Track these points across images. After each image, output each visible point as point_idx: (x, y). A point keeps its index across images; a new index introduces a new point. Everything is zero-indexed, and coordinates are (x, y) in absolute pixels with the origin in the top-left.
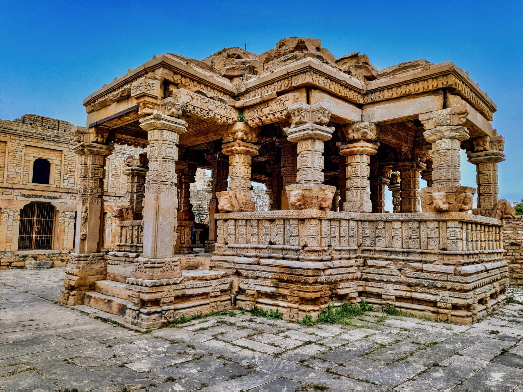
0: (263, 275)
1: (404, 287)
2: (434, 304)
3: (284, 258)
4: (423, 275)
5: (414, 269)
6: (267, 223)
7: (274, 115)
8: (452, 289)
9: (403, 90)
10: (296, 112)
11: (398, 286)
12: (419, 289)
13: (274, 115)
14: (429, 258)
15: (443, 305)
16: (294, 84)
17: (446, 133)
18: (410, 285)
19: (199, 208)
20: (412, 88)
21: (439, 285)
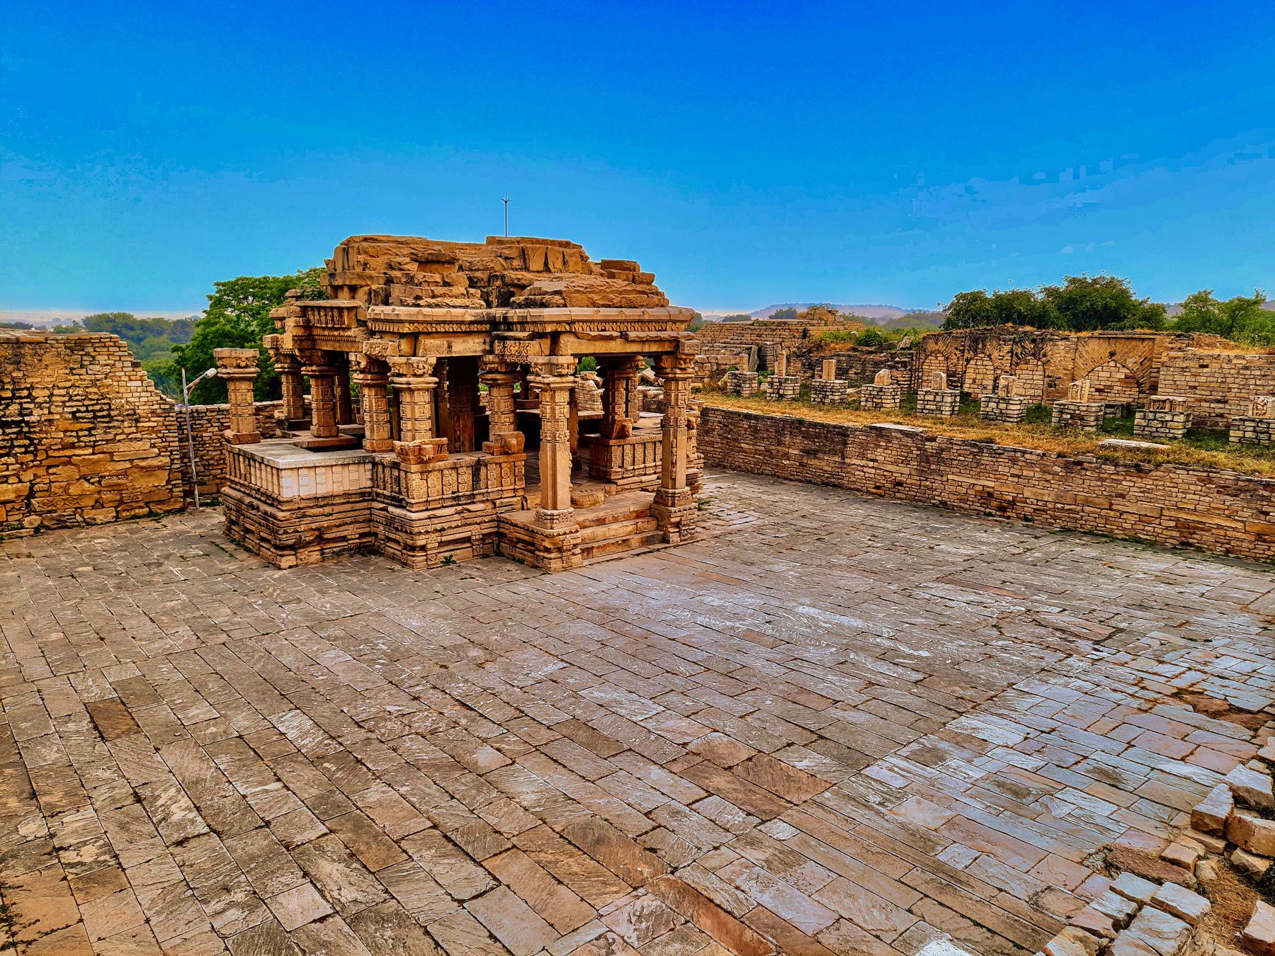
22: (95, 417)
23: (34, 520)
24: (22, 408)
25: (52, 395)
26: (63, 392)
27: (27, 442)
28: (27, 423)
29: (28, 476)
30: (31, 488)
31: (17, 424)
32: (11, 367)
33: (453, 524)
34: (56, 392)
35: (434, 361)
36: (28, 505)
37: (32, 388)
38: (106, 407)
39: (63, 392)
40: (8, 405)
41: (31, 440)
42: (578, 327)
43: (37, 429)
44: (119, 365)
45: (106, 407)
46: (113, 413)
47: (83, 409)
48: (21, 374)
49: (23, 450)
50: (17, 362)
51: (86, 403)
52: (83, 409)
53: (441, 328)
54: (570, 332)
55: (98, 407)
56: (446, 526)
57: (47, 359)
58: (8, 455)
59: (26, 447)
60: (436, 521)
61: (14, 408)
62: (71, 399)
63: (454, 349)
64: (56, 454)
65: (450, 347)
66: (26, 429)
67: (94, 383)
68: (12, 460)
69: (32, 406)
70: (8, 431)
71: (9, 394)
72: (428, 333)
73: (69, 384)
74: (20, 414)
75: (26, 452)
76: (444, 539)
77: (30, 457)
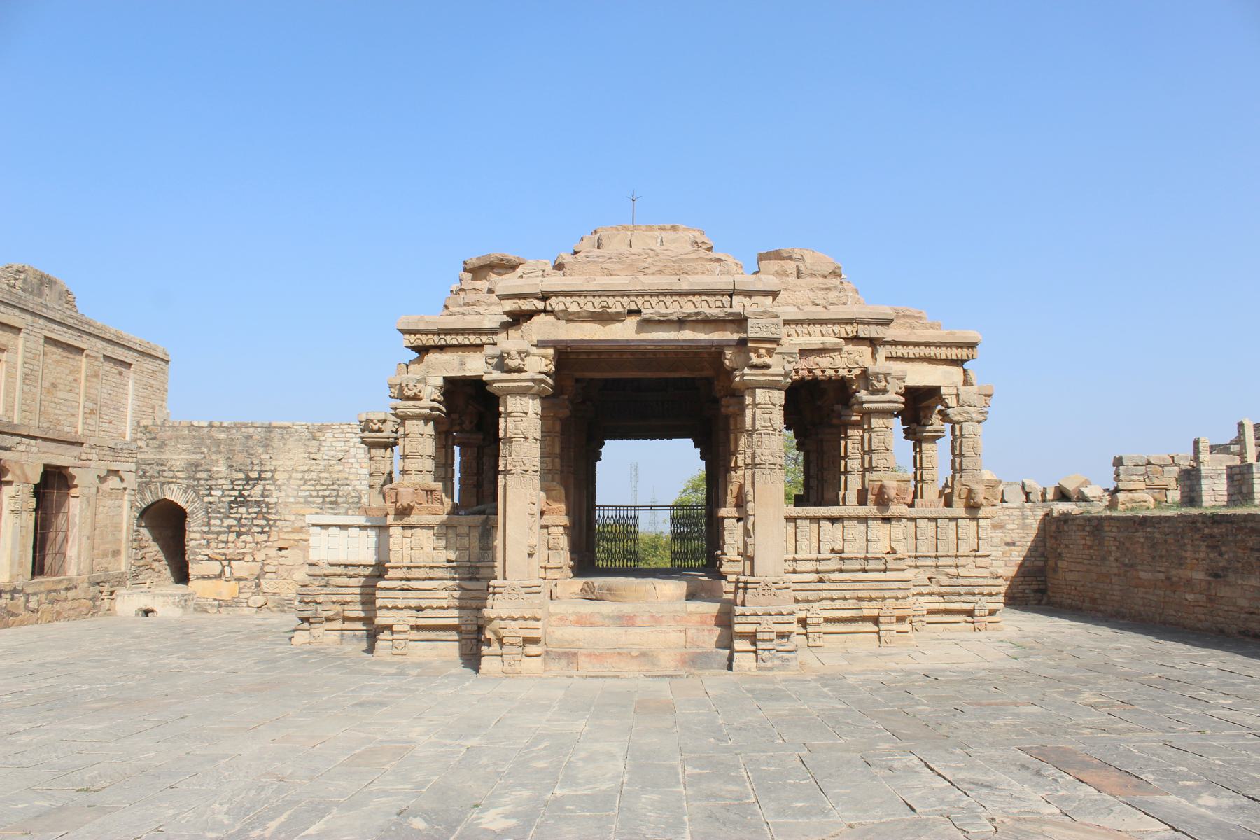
0: (835, 595)
1: (936, 598)
2: (970, 613)
3: (865, 571)
4: (961, 581)
5: (951, 576)
6: (829, 524)
7: (837, 372)
8: (990, 595)
9: (923, 351)
10: (882, 377)
11: (928, 598)
12: (956, 598)
13: (837, 372)
14: (961, 561)
15: (982, 613)
16: (861, 335)
17: (974, 415)
18: (942, 595)
19: (196, 472)
20: (932, 351)
21: (976, 590)
22: (323, 502)
23: (260, 600)
24: (265, 490)
25: (290, 478)
26: (300, 476)
27: (264, 522)
28: (267, 504)
29: (260, 556)
30: (262, 568)
31: (258, 503)
32: (261, 450)
33: (435, 603)
34: (295, 475)
35: (440, 382)
36: (258, 585)
37: (274, 471)
38: (335, 493)
39: (300, 476)
40: (254, 486)
41: (268, 520)
42: (554, 303)
43: (274, 511)
44: (353, 451)
45: (335, 493)
46: (340, 500)
47: (315, 494)
48: (268, 457)
49: (259, 529)
50: (266, 444)
51: (318, 487)
52: (315, 494)
53: (451, 340)
54: (545, 311)
55: (327, 493)
56: (424, 603)
57: (291, 443)
58: (248, 533)
59: (263, 527)
60: (410, 594)
61: (259, 489)
62: (305, 484)
63: (468, 366)
64: (286, 537)
65: (463, 364)
66: (265, 510)
67: (327, 468)
68: (249, 538)
69: (272, 488)
70: (251, 510)
71: (256, 475)
72: (441, 348)
73: (305, 468)
74: (263, 495)
75: (262, 532)
76: (421, 622)
77: (264, 537)
